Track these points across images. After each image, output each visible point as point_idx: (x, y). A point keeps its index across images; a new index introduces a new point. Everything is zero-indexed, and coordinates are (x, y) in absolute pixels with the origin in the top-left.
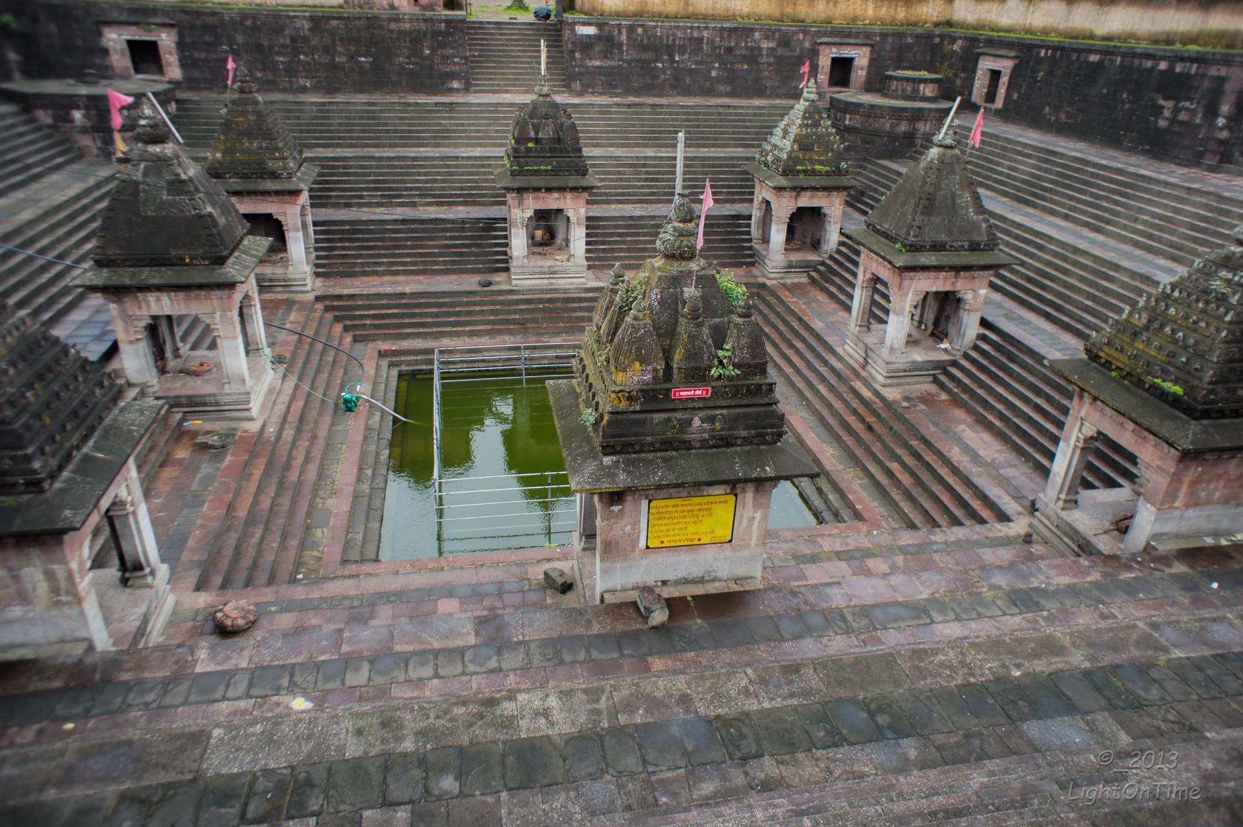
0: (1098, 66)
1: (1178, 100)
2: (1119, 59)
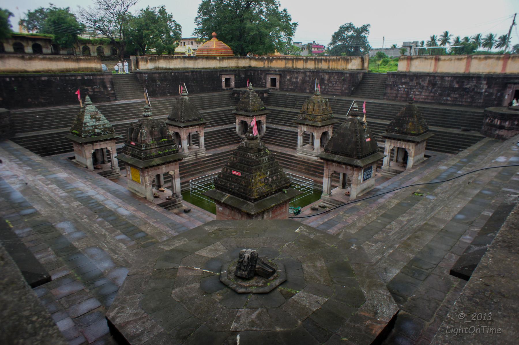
0: (48, 81)
1: (92, 86)
2: (58, 78)
